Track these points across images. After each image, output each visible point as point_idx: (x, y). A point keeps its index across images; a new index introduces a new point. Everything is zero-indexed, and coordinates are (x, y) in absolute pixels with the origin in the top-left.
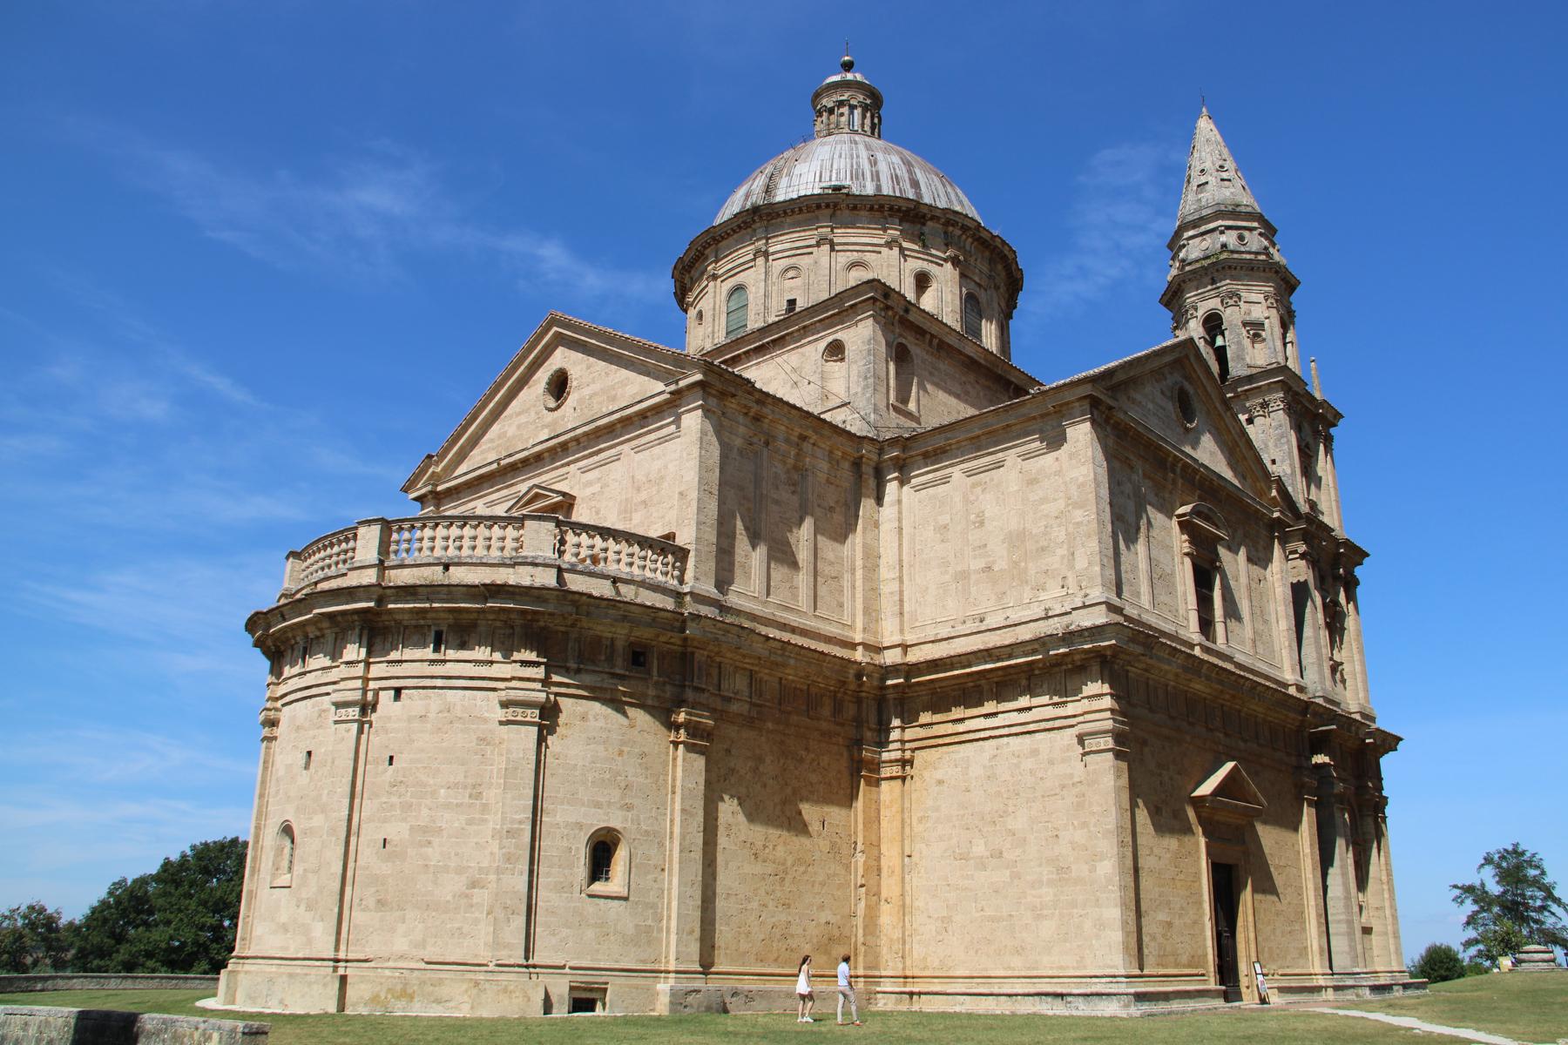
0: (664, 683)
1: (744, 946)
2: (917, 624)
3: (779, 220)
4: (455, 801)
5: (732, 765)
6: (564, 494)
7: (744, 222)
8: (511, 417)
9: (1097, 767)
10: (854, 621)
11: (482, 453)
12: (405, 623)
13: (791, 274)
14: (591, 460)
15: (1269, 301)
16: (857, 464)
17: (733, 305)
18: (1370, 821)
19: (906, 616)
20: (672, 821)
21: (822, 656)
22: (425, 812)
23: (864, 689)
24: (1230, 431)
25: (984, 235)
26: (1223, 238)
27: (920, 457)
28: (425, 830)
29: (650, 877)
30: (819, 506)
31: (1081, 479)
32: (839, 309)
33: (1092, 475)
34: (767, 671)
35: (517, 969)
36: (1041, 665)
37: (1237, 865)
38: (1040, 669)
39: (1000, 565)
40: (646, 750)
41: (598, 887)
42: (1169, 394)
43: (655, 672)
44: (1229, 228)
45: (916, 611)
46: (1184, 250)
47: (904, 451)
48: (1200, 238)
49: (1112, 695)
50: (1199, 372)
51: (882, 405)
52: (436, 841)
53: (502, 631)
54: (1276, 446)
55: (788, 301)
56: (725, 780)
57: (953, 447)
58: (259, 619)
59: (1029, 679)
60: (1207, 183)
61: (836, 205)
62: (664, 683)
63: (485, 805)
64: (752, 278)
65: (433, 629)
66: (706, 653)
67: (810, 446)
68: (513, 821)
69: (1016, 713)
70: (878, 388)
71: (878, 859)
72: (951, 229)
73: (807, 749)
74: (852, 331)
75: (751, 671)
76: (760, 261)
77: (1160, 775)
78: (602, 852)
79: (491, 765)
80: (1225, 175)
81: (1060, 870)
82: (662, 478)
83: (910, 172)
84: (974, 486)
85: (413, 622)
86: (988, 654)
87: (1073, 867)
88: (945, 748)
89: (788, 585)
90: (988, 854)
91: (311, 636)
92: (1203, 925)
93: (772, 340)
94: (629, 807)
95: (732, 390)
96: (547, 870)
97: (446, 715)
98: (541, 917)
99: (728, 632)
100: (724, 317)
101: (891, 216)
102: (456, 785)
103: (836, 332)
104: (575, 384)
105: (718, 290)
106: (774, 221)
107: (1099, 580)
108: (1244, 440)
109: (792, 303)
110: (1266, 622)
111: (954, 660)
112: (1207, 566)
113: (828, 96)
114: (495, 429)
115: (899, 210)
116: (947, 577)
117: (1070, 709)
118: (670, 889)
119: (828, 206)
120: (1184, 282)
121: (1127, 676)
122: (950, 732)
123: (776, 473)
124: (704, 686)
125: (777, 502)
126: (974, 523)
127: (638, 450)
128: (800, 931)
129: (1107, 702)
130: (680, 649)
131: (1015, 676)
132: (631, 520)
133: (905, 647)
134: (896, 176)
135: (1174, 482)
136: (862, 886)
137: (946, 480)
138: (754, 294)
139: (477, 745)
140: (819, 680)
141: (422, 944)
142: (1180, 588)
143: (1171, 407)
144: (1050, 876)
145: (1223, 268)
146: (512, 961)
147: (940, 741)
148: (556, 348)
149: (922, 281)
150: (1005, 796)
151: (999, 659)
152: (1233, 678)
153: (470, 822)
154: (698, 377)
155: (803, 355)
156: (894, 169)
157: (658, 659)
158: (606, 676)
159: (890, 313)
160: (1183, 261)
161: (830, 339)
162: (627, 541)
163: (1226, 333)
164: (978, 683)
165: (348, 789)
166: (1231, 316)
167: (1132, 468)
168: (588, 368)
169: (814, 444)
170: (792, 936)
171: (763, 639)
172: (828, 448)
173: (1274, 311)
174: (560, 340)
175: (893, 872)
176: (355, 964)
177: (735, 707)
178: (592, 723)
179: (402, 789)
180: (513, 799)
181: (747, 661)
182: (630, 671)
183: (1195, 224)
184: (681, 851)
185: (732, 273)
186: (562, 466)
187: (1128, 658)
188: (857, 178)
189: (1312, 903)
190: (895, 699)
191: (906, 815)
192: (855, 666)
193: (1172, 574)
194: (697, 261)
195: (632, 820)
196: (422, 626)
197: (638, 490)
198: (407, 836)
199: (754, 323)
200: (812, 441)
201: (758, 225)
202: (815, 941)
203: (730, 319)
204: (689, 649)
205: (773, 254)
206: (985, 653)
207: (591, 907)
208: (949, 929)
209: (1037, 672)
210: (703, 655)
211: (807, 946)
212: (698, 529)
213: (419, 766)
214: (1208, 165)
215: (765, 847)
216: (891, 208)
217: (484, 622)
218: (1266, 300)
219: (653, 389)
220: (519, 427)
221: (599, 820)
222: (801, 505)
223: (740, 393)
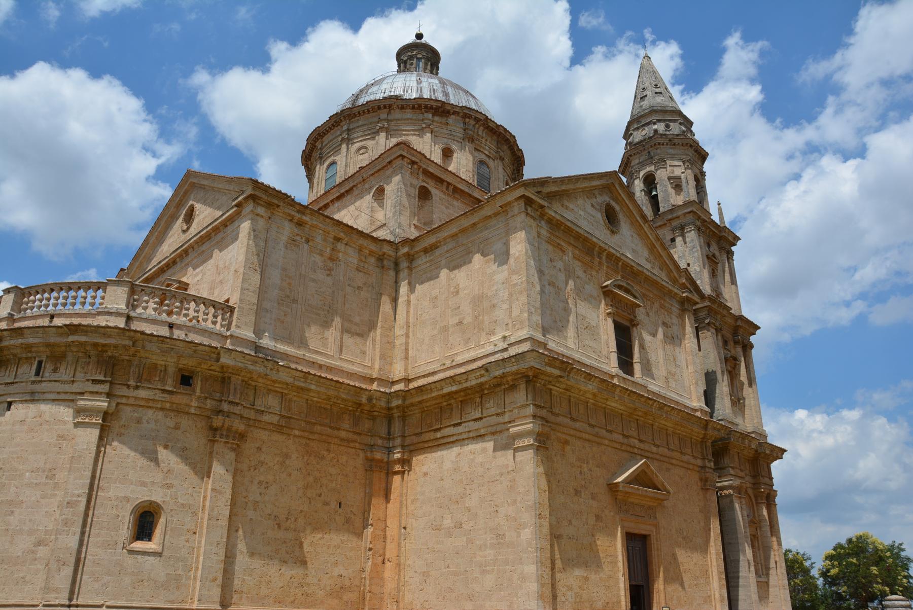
1: (264, 591)
2: (416, 365)
3: (356, 118)
4: (35, 481)
5: (262, 459)
7: (335, 122)
9: (523, 458)
10: (373, 364)
12: (20, 356)
16: (381, 259)
17: (329, 175)
19: (410, 359)
20: (205, 497)
21: (338, 384)
22: (13, 489)
23: (375, 409)
24: (648, 237)
25: (491, 124)
26: (655, 127)
27: (422, 253)
29: (183, 538)
30: (349, 285)
33: (524, 250)
34: (295, 394)
37: (649, 535)
38: (488, 389)
39: (468, 320)
40: (187, 446)
41: (139, 545)
42: (598, 207)
43: (198, 390)
44: (659, 121)
45: (416, 356)
50: (622, 195)
52: (17, 511)
53: (84, 360)
54: (690, 254)
56: (255, 469)
57: (442, 243)
59: (481, 397)
60: (646, 96)
61: (390, 106)
62: (206, 398)
65: (37, 359)
67: (343, 246)
69: (473, 423)
71: (384, 531)
72: (467, 120)
73: (328, 450)
75: (282, 393)
77: (581, 467)
79: (65, 454)
80: (657, 90)
81: (498, 536)
85: (24, 355)
89: (320, 337)
90: (452, 525)
92: (618, 579)
94: (169, 486)
95: (276, 202)
96: (97, 531)
97: (38, 419)
99: (256, 362)
101: (426, 112)
104: (197, 213)
107: (527, 323)
108: (659, 243)
110: (677, 366)
111: (433, 386)
112: (627, 324)
115: (431, 107)
116: (435, 332)
118: (199, 547)
119: (385, 107)
121: (551, 393)
122: (432, 438)
123: (315, 261)
124: (237, 401)
125: (314, 280)
126: (453, 293)
128: (315, 581)
130: (221, 375)
131: (472, 396)
133: (407, 380)
134: (434, 90)
136: (370, 549)
139: (57, 440)
140: (339, 402)
142: (603, 337)
143: (600, 217)
144: (492, 541)
145: (655, 144)
149: (447, 153)
150: (465, 483)
152: (643, 400)
156: (433, 86)
157: (201, 381)
158: (158, 392)
159: (416, 166)
163: (658, 186)
164: (450, 402)
166: (661, 175)
167: (563, 252)
169: (346, 244)
170: (308, 584)
172: (357, 247)
175: (393, 539)
177: (266, 418)
181: (277, 385)
184: (209, 519)
187: (547, 378)
188: (407, 91)
189: (714, 564)
190: (398, 416)
191: (404, 498)
192: (367, 393)
193: (597, 326)
194: (313, 151)
195: (171, 496)
196: (31, 358)
201: (344, 123)
202: (328, 588)
203: (327, 183)
204: (226, 375)
206: (450, 379)
207: (130, 560)
208: (428, 581)
209: (486, 392)
210: (238, 379)
211: (321, 592)
212: (242, 293)
213: (15, 456)
215: (287, 519)
216: (426, 107)
217: (71, 354)
221: (142, 495)
223: (281, 204)
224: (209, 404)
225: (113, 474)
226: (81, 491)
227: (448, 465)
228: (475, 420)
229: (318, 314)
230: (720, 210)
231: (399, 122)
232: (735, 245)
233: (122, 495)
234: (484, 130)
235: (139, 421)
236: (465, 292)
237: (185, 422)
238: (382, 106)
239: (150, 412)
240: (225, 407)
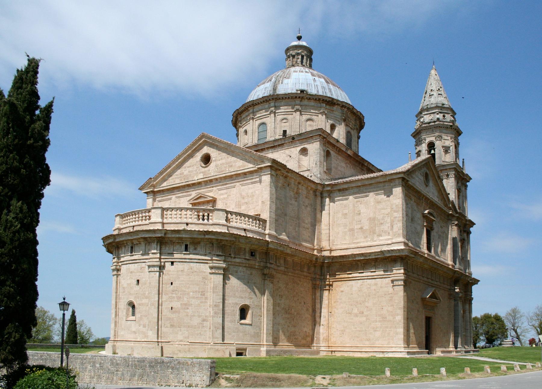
0: (261, 262)
3: (280, 100)
7: (266, 100)
13: (284, 121)
14: (223, 187)
15: (452, 139)
16: (315, 191)
24: (439, 186)
25: (355, 111)
28: (186, 304)
30: (303, 205)
35: (220, 344)
36: (380, 259)
39: (366, 227)
46: (423, 119)
47: (332, 188)
51: (322, 172)
58: (111, 236)
63: (206, 297)
64: (269, 120)
66: (273, 253)
67: (301, 186)
68: (216, 302)
70: (321, 166)
72: (344, 108)
74: (311, 145)
76: (273, 115)
78: (243, 312)
84: (357, 202)
91: (134, 243)
93: (276, 145)
98: (226, 330)
101: (322, 103)
102: (196, 291)
103: (305, 145)
104: (213, 159)
106: (278, 101)
109: (285, 132)
113: (293, 50)
120: (422, 130)
125: (291, 204)
126: (357, 214)
127: (242, 185)
132: (241, 208)
134: (324, 87)
135: (422, 202)
137: (347, 199)
141: (188, 337)
145: (437, 127)
146: (218, 342)
149: (333, 127)
153: (201, 302)
155: (291, 151)
157: (259, 254)
160: (422, 122)
161: (302, 147)
162: (240, 215)
165: (157, 292)
169: (302, 185)
171: (290, 248)
173: (453, 143)
174: (206, 143)
176: (164, 343)
179: (177, 292)
180: (216, 296)
182: (250, 258)
183: (428, 109)
185: (260, 118)
186: (210, 187)
197: (243, 198)
198: (180, 306)
200: (302, 184)
205: (277, 113)
218: (451, 139)
222: (298, 205)
225: (230, 294)
226: (219, 301)
229: (293, 220)
231: (307, 107)
232: (469, 182)
234: (350, 113)
235: (237, 272)
236: (364, 214)
237: (254, 272)
238: (298, 97)
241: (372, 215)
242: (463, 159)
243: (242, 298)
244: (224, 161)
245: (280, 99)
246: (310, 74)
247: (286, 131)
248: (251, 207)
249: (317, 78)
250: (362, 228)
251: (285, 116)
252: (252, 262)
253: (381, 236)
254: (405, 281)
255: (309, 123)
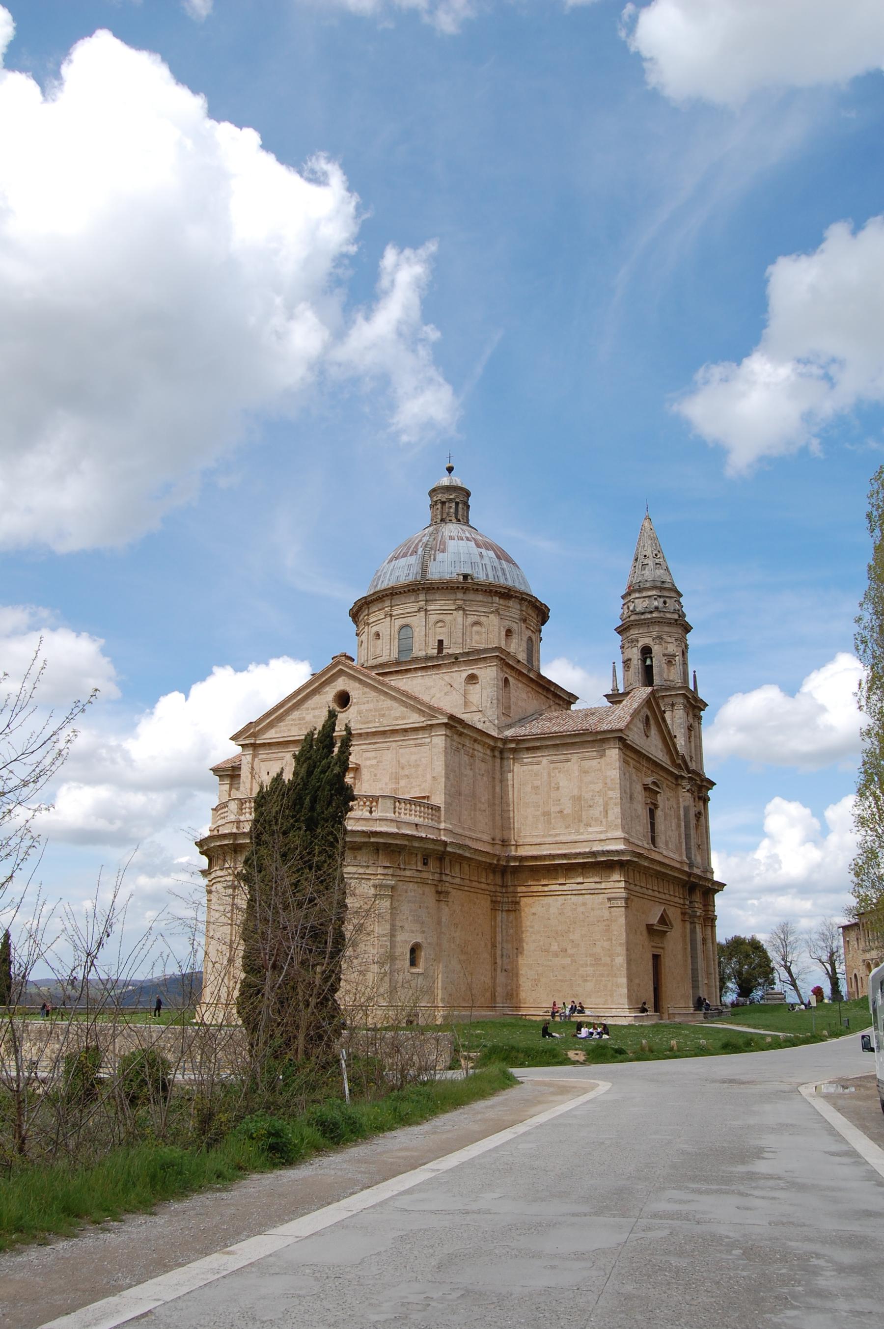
6: (356, 764)
8: (308, 709)
11: (286, 726)
13: (440, 624)
18: (709, 928)
31: (613, 777)
32: (473, 657)
48: (643, 599)
49: (625, 881)
55: (439, 640)
82: (418, 766)
83: (500, 563)
84: (554, 769)
86: (564, 856)
87: (603, 959)
88: (537, 898)
100: (397, 641)
101: (495, 596)
104: (355, 700)
105: (393, 624)
114: (296, 714)
116: (539, 813)
117: (603, 886)
126: (554, 788)
129: (622, 884)
138: (418, 632)
147: (535, 894)
148: (339, 676)
151: (569, 859)
154: (446, 721)
155: (452, 677)
161: (470, 672)
168: (363, 694)
178: (409, 894)
197: (403, 768)
199: (418, 651)
205: (429, 611)
214: (648, 553)
219: (415, 719)
220: (314, 717)
224: (437, 877)
227: (553, 910)
228: (578, 883)
229: (468, 801)
230: (695, 677)
233: (403, 939)
239: (411, 884)
240: (444, 878)
241: (576, 792)
242: (695, 672)
243: (413, 932)
244: (371, 706)
245: (433, 588)
246: (472, 544)
247: (442, 640)
248: (414, 783)
249: (483, 551)
250: (561, 812)
251: (441, 617)
252: (424, 875)
253: (590, 826)
254: (627, 899)
255: (475, 628)
